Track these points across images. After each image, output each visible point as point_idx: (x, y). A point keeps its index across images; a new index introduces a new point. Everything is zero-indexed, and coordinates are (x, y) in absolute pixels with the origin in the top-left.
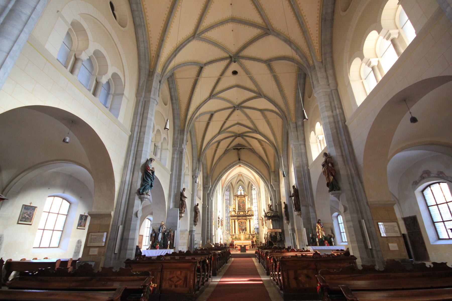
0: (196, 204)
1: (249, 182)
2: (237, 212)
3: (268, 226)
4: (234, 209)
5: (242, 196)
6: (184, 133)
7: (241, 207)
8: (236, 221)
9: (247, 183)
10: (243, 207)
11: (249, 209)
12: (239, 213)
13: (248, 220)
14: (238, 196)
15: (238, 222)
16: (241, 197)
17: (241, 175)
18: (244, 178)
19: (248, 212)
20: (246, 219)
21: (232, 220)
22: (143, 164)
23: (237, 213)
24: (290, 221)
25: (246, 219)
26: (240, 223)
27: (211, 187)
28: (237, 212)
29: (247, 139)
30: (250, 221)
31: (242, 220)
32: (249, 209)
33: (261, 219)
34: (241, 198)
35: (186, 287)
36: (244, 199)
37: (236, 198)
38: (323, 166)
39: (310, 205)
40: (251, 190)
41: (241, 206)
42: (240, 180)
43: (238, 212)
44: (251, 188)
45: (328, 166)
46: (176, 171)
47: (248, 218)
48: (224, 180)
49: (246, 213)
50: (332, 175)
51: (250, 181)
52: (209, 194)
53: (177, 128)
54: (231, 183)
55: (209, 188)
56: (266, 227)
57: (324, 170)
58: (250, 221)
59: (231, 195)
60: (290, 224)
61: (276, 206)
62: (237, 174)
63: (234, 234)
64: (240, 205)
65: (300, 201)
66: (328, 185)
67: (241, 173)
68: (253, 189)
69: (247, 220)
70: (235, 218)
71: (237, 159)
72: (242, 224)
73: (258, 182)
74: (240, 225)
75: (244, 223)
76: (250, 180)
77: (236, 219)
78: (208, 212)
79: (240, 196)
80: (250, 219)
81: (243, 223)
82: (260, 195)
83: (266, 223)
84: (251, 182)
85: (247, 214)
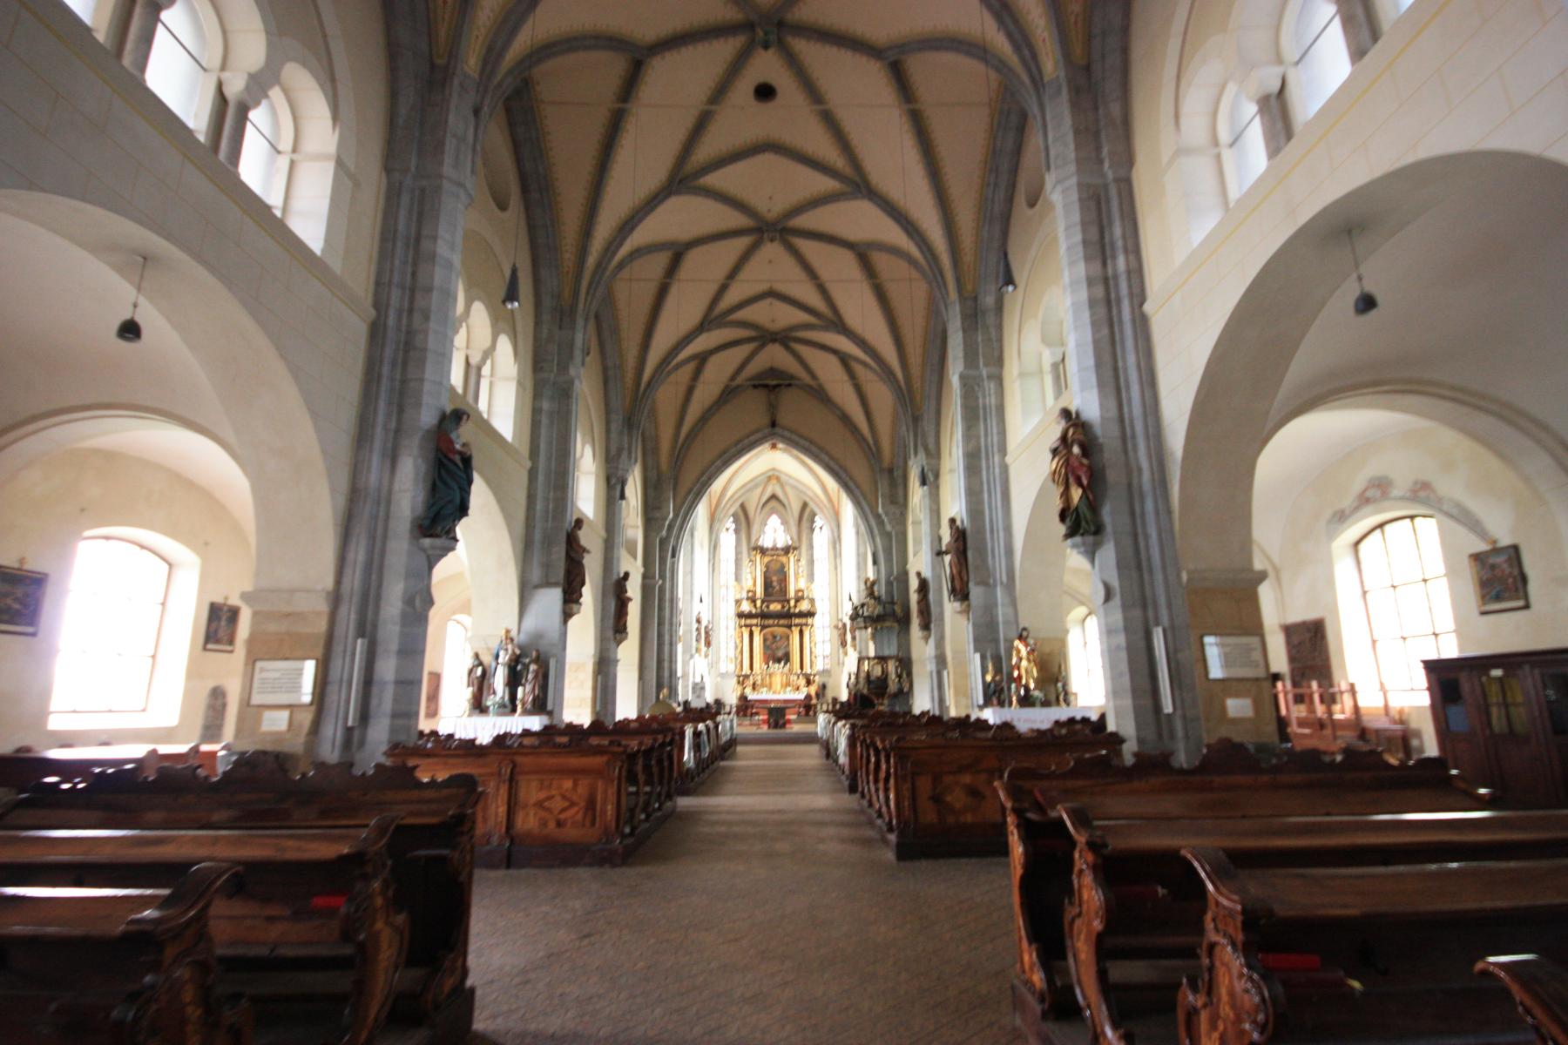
0: (622, 575)
1: (805, 505)
2: (759, 603)
3: (860, 647)
6: (573, 321)
8: (756, 631)
9: (796, 507)
10: (780, 585)
12: (768, 607)
13: (796, 631)
14: (763, 551)
15: (764, 635)
17: (778, 479)
18: (789, 490)
20: (789, 627)
21: (744, 628)
22: (428, 431)
23: (761, 607)
24: (933, 632)
25: (789, 627)
26: (770, 637)
27: (671, 515)
28: (759, 603)
29: (804, 350)
30: (801, 633)
31: (776, 629)
33: (840, 625)
35: (593, 823)
36: (784, 559)
38: (1055, 452)
39: (1002, 583)
41: (775, 584)
42: (774, 497)
43: (763, 602)
45: (1070, 451)
46: (549, 459)
47: (797, 621)
49: (790, 608)
50: (1080, 484)
51: (808, 500)
52: (663, 542)
53: (547, 302)
54: (743, 506)
55: (666, 519)
56: (855, 650)
57: (1054, 466)
58: (801, 633)
60: (932, 641)
61: (889, 583)
62: (763, 474)
63: (749, 672)
64: (771, 582)
65: (971, 568)
66: (1063, 516)
67: (777, 473)
70: (754, 621)
71: (767, 421)
73: (836, 504)
75: (784, 640)
76: (808, 496)
77: (756, 625)
78: (661, 600)
80: (801, 625)
81: (778, 638)
82: (840, 546)
83: (854, 638)
84: (811, 505)
85: (792, 610)
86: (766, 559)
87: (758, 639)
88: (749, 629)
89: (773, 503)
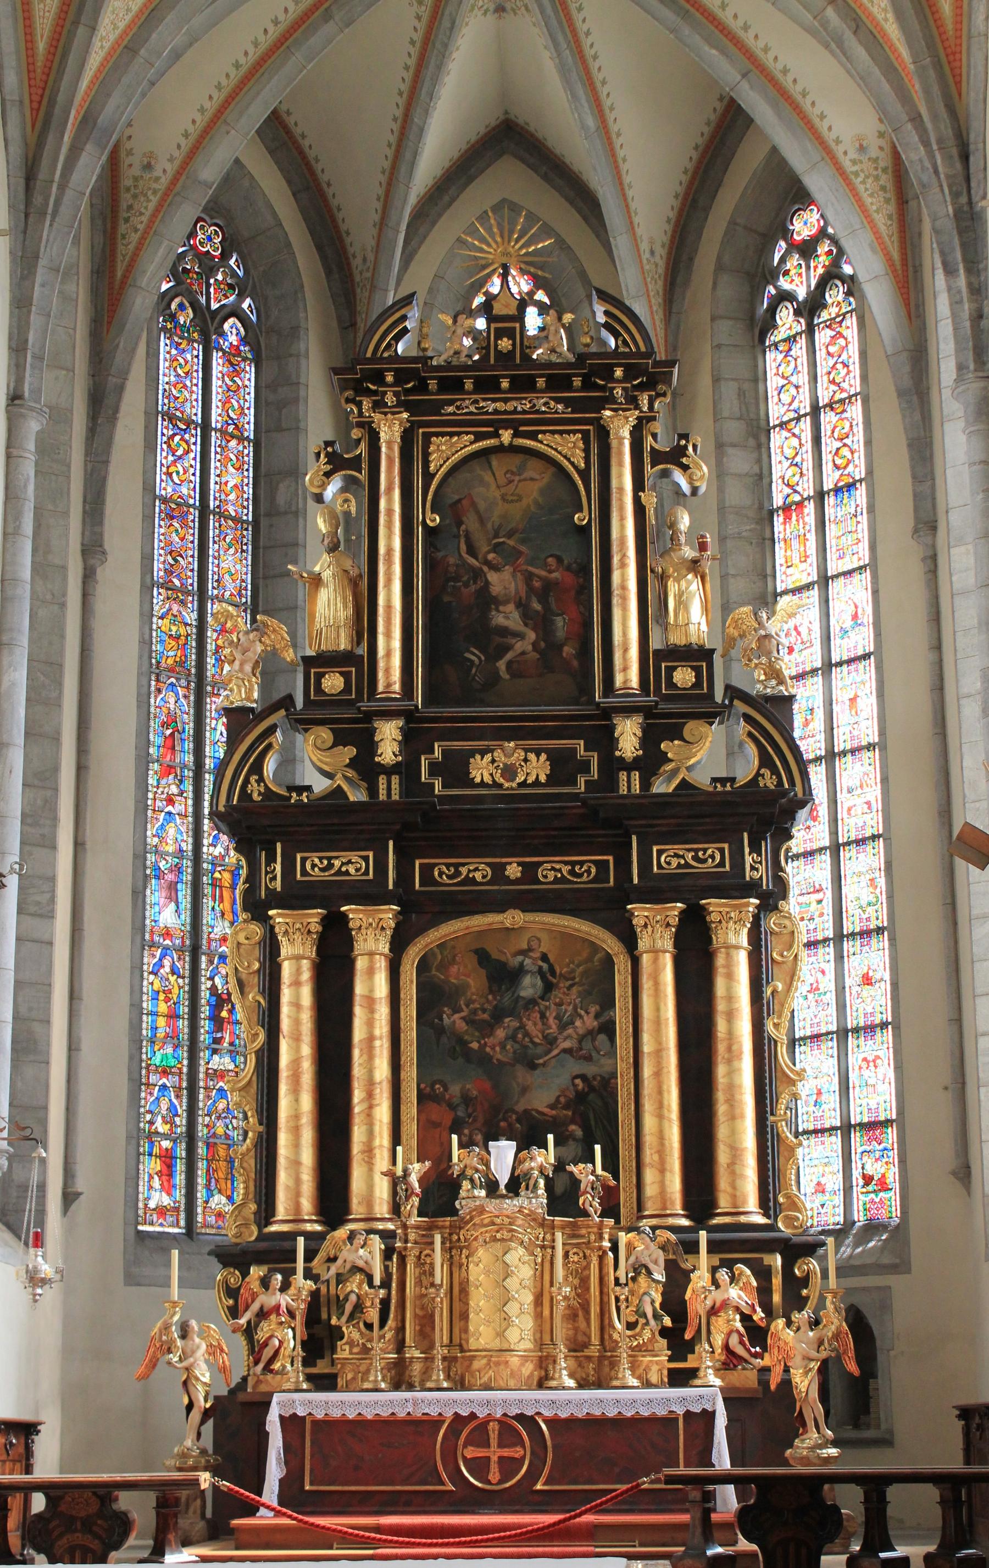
4: (333, 683)
5: (523, 385)
10: (543, 624)
11: (684, 676)
15: (423, 967)
19: (669, 747)
31: (513, 918)
32: (684, 676)
34: (515, 426)
40: (729, 331)
44: (730, 289)
64: (486, 600)
68: (787, 320)
69: (640, 912)
72: (498, 1016)
74: (454, 1020)
79: (487, 385)
81: (529, 986)
88: (313, 917)
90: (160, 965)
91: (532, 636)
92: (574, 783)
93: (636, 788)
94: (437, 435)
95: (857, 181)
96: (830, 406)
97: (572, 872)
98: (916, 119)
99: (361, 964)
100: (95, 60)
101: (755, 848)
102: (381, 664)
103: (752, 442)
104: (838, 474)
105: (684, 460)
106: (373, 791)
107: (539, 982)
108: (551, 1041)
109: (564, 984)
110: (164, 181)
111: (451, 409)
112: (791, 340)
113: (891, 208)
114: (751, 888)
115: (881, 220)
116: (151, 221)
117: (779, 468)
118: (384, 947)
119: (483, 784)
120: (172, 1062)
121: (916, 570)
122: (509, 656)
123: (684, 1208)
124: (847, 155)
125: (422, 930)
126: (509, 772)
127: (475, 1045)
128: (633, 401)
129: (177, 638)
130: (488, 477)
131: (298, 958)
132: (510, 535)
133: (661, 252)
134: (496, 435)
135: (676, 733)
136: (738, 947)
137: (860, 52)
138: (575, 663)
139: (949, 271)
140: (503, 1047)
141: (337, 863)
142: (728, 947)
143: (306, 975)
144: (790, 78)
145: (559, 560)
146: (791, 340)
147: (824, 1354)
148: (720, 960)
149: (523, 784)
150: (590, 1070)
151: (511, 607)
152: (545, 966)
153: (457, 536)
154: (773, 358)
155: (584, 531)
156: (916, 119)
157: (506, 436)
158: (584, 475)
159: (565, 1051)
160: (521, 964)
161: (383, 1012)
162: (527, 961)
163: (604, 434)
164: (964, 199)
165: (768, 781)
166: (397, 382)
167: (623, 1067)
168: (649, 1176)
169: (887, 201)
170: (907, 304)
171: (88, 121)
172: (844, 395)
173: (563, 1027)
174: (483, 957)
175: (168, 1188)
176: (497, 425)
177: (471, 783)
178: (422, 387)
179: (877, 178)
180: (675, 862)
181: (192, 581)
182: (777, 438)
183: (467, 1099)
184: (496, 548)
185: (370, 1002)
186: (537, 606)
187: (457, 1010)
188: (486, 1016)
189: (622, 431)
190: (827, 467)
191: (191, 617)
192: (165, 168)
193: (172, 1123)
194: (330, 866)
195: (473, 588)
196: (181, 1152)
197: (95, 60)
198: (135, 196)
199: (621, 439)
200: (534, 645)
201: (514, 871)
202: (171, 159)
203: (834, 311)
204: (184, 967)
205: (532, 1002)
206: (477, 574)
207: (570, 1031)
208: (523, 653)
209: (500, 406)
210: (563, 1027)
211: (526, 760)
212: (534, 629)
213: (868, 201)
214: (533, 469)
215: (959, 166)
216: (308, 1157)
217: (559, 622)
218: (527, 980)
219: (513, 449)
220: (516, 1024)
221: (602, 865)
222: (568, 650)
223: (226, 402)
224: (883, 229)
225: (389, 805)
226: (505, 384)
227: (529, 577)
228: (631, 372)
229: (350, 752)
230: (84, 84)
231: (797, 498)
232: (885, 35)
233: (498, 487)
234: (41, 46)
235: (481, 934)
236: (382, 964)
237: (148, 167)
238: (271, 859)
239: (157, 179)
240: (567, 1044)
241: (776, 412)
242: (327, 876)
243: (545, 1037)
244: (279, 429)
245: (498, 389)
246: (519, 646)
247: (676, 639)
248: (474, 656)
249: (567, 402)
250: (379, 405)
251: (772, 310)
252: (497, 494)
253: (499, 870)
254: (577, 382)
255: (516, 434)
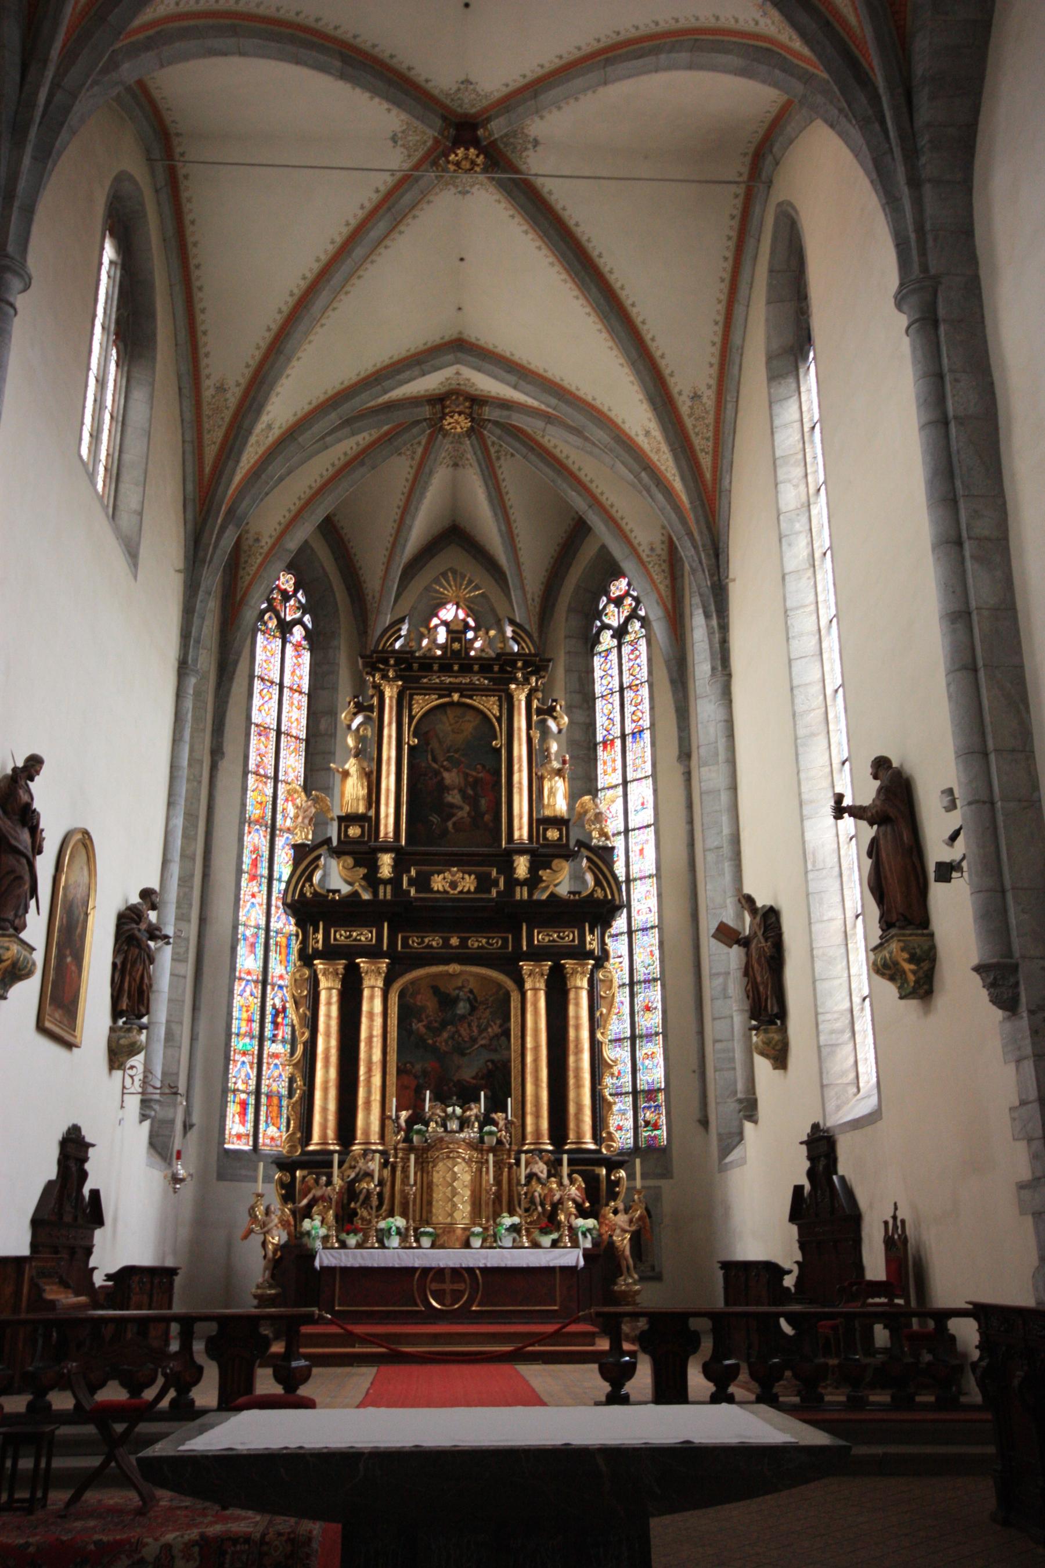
2: (386, 861)
4: (354, 831)
7: (446, 811)
11: (553, 834)
12: (422, 883)
15: (402, 995)
16: (462, 690)
19: (545, 874)
23: (395, 882)
26: (428, 1002)
28: (386, 861)
31: (454, 968)
32: (553, 834)
33: (747, 924)
34: (462, 690)
36: (490, 706)
37: (390, 693)
41: (454, 798)
48: (233, 396)
49: (512, 882)
59: (334, 688)
64: (442, 788)
68: (607, 640)
69: (526, 966)
70: (365, 936)
72: (444, 1025)
73: (706, 461)
77: (373, 953)
79: (445, 668)
80: (555, 954)
81: (462, 1008)
86: (421, 705)
87: (372, 1004)
88: (341, 965)
89: (452, 557)
90: (244, 991)
91: (467, 808)
92: (490, 892)
93: (525, 896)
94: (417, 694)
95: (650, 566)
96: (630, 687)
97: (488, 943)
98: (690, 534)
99: (366, 993)
100: (237, 478)
101: (592, 932)
102: (382, 822)
103: (585, 705)
104: (634, 725)
105: (555, 714)
106: (375, 893)
107: (468, 1005)
108: (474, 1040)
109: (482, 1007)
110: (266, 549)
111: (425, 680)
112: (608, 651)
113: (668, 582)
114: (590, 954)
115: (662, 587)
116: (258, 569)
117: (600, 720)
118: (380, 983)
119: (438, 891)
120: (249, 1048)
121: (679, 779)
122: (454, 819)
123: (550, 1138)
124: (644, 551)
125: (401, 974)
126: (453, 885)
127: (430, 1041)
128: (527, 681)
129: (261, 803)
130: (444, 719)
131: (330, 989)
132: (456, 751)
133: (537, 599)
134: (450, 696)
135: (548, 866)
136: (582, 988)
137: (660, 497)
138: (491, 825)
139: (707, 616)
140: (446, 1042)
141: (355, 934)
142: (577, 988)
143: (335, 999)
144: (614, 509)
145: (484, 767)
146: (608, 651)
147: (633, 1228)
148: (572, 995)
149: (461, 892)
150: (495, 1057)
151: (456, 791)
152: (471, 997)
153: (426, 751)
154: (597, 661)
155: (498, 751)
156: (690, 534)
157: (456, 697)
158: (499, 720)
159: (482, 1046)
160: (458, 995)
161: (378, 1021)
162: (461, 994)
163: (510, 698)
164: (716, 578)
165: (599, 894)
166: (397, 664)
167: (514, 1055)
168: (529, 1120)
169: (666, 578)
170: (676, 634)
171: (231, 512)
172: (638, 682)
173: (481, 1032)
174: (436, 990)
175: (243, 1122)
176: (449, 690)
177: (431, 891)
178: (410, 668)
179: (660, 565)
180: (547, 939)
181: (271, 772)
182: (599, 704)
183: (425, 1073)
184: (448, 759)
185: (371, 1015)
186: (470, 792)
187: (420, 1021)
188: (436, 1025)
189: (521, 697)
190: (628, 721)
191: (269, 791)
192: (266, 542)
193: (247, 1083)
194: (350, 936)
195: (435, 780)
196: (252, 1101)
197: (237, 478)
198: (249, 556)
199: (520, 701)
200: (469, 813)
201: (454, 941)
202: (271, 537)
203: (633, 636)
204: (258, 992)
205: (463, 1017)
206: (437, 773)
207: (484, 1035)
208: (462, 818)
209: (452, 680)
210: (481, 1032)
211: (463, 878)
212: (469, 804)
213: (656, 577)
214: (470, 716)
215: (713, 560)
216: (332, 1106)
217: (483, 802)
218: (461, 1004)
219: (459, 704)
220: (453, 1029)
221: (505, 940)
222: (487, 817)
223: (293, 672)
224: (663, 593)
225: (385, 902)
226: (456, 668)
227: (466, 775)
228: (526, 664)
229: (362, 871)
230: (230, 492)
231: (611, 737)
232: (673, 488)
233: (451, 725)
234: (207, 470)
235: (435, 976)
236: (378, 993)
237: (257, 540)
238: (316, 931)
239: (262, 547)
240: (483, 1042)
241: (598, 689)
242: (348, 942)
243: (471, 1037)
244: (323, 688)
245: (452, 671)
246: (460, 814)
247: (548, 812)
248: (435, 819)
249: (490, 679)
250: (384, 677)
251: (598, 634)
252: (449, 728)
253: (446, 941)
254: (496, 668)
255: (461, 696)
